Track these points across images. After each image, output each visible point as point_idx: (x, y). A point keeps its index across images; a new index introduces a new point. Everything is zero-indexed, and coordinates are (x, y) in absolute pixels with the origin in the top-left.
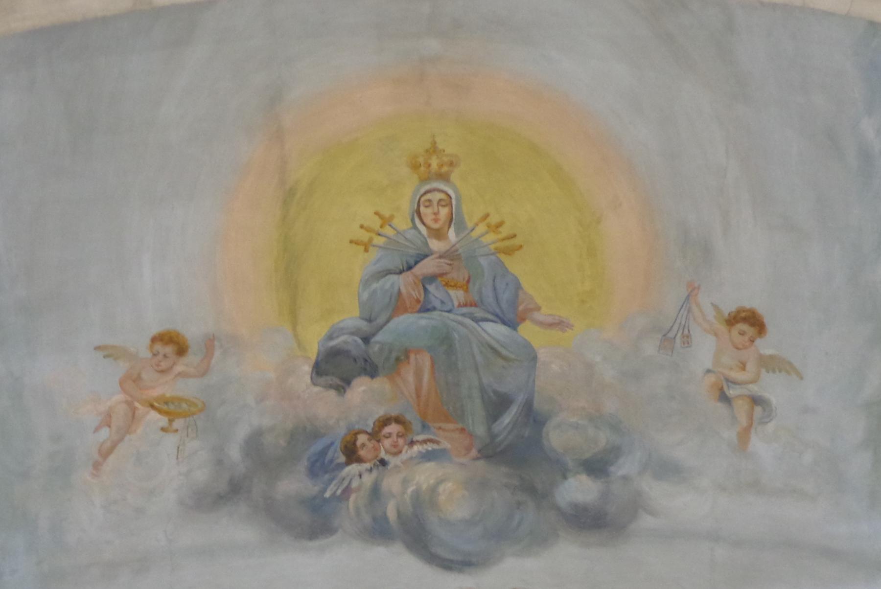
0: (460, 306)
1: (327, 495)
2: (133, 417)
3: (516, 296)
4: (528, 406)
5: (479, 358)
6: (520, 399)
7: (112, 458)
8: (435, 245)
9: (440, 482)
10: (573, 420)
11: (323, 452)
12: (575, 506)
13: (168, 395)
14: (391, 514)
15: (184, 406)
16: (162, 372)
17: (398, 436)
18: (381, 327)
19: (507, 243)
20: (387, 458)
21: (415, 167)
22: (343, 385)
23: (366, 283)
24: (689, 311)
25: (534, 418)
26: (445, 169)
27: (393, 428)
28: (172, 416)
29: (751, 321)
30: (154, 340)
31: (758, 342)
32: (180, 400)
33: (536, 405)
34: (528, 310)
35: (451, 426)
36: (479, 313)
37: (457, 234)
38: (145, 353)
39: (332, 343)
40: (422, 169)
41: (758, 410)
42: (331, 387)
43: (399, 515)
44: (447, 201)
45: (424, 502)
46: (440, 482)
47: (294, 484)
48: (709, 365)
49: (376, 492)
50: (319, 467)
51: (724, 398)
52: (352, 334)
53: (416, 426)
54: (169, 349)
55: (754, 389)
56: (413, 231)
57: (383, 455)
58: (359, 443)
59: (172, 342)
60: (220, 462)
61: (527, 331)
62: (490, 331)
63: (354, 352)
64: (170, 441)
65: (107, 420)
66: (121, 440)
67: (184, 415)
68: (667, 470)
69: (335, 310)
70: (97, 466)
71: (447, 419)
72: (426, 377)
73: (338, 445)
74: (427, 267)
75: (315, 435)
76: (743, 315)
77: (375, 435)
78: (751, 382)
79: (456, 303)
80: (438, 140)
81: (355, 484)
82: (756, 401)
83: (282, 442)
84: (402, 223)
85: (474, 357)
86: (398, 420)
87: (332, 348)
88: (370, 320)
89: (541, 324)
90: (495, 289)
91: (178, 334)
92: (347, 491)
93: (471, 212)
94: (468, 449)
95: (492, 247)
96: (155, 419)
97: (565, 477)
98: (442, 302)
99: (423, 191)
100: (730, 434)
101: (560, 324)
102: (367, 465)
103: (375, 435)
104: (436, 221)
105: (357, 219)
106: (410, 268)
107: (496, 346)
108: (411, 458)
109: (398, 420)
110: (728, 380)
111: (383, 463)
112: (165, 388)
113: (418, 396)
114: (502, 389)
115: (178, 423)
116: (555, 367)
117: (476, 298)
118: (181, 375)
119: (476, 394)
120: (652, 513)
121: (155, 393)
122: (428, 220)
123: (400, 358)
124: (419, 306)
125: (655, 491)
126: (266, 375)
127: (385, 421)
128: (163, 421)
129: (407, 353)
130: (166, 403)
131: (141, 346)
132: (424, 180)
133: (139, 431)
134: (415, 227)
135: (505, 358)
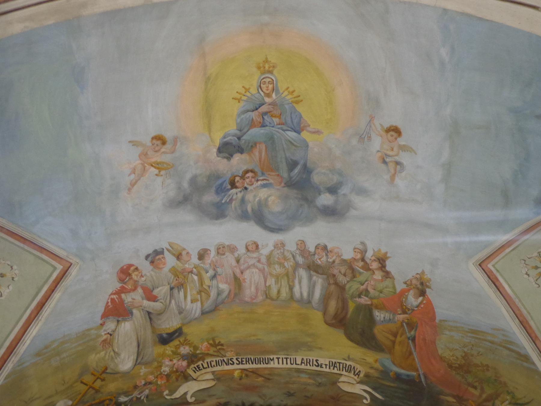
0: (277, 124)
1: (223, 201)
2: (144, 170)
3: (300, 120)
4: (305, 166)
5: (285, 146)
6: (302, 162)
7: (135, 186)
8: (267, 100)
9: (269, 196)
10: (323, 171)
11: (222, 184)
13: (158, 161)
14: (249, 209)
15: (165, 165)
16: (156, 151)
17: (252, 178)
18: (245, 133)
19: (296, 99)
20: (247, 186)
21: (259, 68)
22: (230, 157)
23: (239, 115)
24: (370, 127)
25: (307, 170)
26: (271, 69)
27: (250, 174)
28: (160, 170)
29: (396, 131)
30: (153, 138)
31: (398, 139)
32: (163, 163)
33: (308, 165)
34: (305, 126)
35: (273, 174)
36: (285, 127)
37: (276, 95)
38: (149, 144)
40: (262, 69)
41: (398, 167)
42: (225, 157)
43: (253, 210)
45: (262, 204)
46: (269, 196)
47: (210, 197)
48: (378, 149)
49: (243, 200)
50: (220, 190)
51: (385, 162)
52: (233, 136)
53: (259, 173)
54: (159, 142)
55: (397, 158)
56: (258, 94)
57: (246, 185)
58: (236, 180)
59: (160, 140)
60: (179, 188)
61: (305, 135)
62: (289, 135)
63: (234, 143)
64: (159, 180)
65: (134, 171)
66: (139, 179)
67: (165, 169)
68: (362, 191)
69: (226, 127)
70: (129, 190)
71: (272, 171)
73: (227, 181)
74: (264, 109)
75: (218, 177)
76: (392, 128)
77: (243, 177)
78: (396, 156)
79: (276, 124)
80: (268, 57)
81: (234, 197)
82: (397, 163)
83: (205, 180)
84: (253, 91)
85: (283, 145)
86: (252, 171)
87: (225, 142)
88: (240, 131)
89: (310, 132)
90: (291, 118)
91: (162, 136)
92: (231, 200)
93: (282, 86)
94: (281, 183)
95: (290, 101)
97: (320, 194)
98: (270, 123)
99: (262, 78)
100: (387, 177)
101: (318, 132)
102: (240, 190)
103: (243, 177)
104: (267, 90)
105: (236, 88)
106: (257, 109)
107: (292, 141)
108: (257, 187)
109: (252, 171)
110: (386, 155)
111: (246, 188)
112: (157, 158)
113: (260, 161)
114: (294, 158)
115: (163, 172)
116: (316, 150)
117: (284, 121)
118: (164, 153)
119: (284, 160)
120: (356, 209)
121: (153, 160)
122: (264, 90)
123: (252, 146)
124: (260, 125)
125: (356, 200)
126: (198, 153)
127: (247, 172)
128: (156, 171)
129: (256, 144)
130: (158, 164)
131: (147, 140)
132: (263, 73)
133: (147, 176)
134: (259, 92)
135: (295, 146)
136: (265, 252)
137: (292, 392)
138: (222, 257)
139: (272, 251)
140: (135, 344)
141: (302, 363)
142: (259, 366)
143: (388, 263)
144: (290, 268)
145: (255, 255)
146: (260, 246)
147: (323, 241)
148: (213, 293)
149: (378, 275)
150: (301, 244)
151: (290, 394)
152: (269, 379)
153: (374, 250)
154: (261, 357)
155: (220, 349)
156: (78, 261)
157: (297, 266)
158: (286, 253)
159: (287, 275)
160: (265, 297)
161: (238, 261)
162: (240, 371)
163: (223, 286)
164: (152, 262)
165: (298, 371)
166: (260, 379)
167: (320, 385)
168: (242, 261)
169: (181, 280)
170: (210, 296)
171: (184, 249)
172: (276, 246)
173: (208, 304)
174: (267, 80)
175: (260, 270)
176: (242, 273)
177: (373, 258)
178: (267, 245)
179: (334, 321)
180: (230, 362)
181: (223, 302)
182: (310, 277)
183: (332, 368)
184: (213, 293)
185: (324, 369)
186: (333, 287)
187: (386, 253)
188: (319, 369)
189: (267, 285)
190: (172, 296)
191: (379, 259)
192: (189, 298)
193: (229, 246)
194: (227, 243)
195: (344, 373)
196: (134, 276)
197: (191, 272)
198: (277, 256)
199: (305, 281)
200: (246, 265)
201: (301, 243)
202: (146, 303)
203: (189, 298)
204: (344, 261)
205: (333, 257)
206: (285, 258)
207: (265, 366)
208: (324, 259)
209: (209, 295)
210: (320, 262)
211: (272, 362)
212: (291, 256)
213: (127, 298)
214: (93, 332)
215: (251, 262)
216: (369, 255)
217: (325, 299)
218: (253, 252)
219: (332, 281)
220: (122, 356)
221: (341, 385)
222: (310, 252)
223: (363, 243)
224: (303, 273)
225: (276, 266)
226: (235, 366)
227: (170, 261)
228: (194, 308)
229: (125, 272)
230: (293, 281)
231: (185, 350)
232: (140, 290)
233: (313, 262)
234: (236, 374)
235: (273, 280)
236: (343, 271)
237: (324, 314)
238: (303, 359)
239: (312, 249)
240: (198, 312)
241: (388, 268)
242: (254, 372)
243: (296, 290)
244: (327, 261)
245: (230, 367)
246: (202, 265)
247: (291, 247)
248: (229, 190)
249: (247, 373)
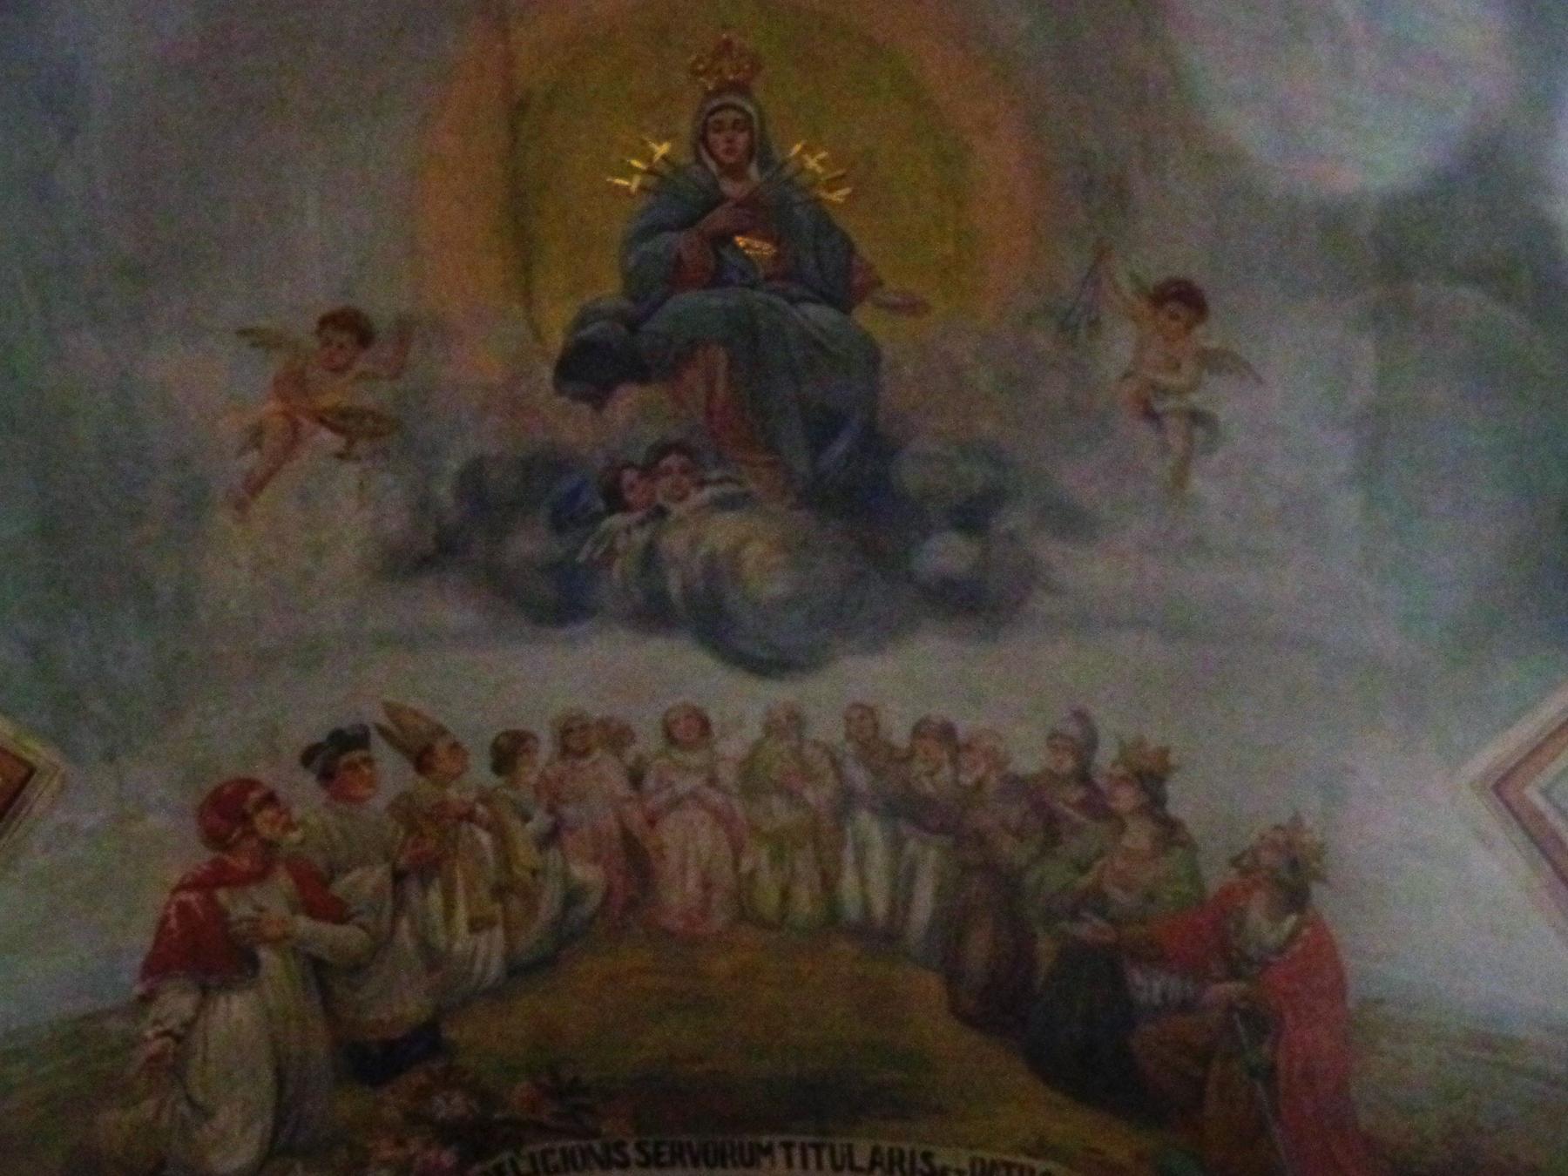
1: (581, 558)
2: (293, 440)
8: (729, 187)
9: (744, 542)
11: (575, 494)
14: (674, 587)
22: (599, 396)
23: (631, 242)
24: (1097, 283)
25: (878, 446)
27: (672, 461)
29: (1182, 300)
31: (1199, 330)
36: (795, 291)
38: (313, 343)
39: (583, 334)
41: (1199, 433)
44: (744, 124)
45: (720, 572)
49: (650, 557)
51: (1151, 415)
54: (345, 337)
55: (1195, 398)
56: (697, 168)
57: (660, 499)
59: (349, 327)
61: (865, 317)
64: (349, 473)
69: (584, 285)
70: (241, 506)
72: (720, 387)
74: (720, 218)
81: (621, 544)
82: (1196, 417)
86: (679, 448)
92: (611, 553)
96: (328, 439)
97: (926, 536)
101: (913, 307)
102: (639, 515)
103: (649, 470)
104: (729, 151)
110: (1154, 386)
113: (710, 413)
115: (362, 446)
118: (362, 376)
121: (328, 400)
127: (663, 450)
131: (304, 329)
134: (699, 160)
136: (732, 747)
139: (758, 746)
140: (267, 1076)
143: (1172, 789)
145: (695, 759)
146: (715, 730)
147: (940, 710)
149: (1139, 835)
150: (863, 722)
156: (56, 760)
157: (847, 800)
158: (808, 751)
161: (636, 778)
163: (585, 872)
164: (326, 776)
168: (650, 783)
169: (430, 845)
171: (442, 731)
172: (770, 728)
173: (532, 938)
174: (731, 116)
175: (716, 814)
176: (652, 823)
177: (1120, 770)
178: (740, 724)
182: (896, 844)
184: (550, 901)
190: (400, 904)
191: (1139, 775)
192: (461, 915)
193: (604, 724)
194: (597, 713)
196: (264, 821)
197: (470, 816)
199: (878, 857)
200: (664, 797)
201: (862, 718)
202: (303, 924)
203: (461, 915)
204: (1017, 785)
205: (975, 765)
206: (808, 774)
209: (531, 900)
210: (929, 788)
212: (825, 764)
213: (239, 906)
214: (115, 1025)
215: (684, 785)
216: (1106, 757)
217: (953, 923)
218: (688, 746)
220: (222, 1118)
223: (1081, 716)
224: (869, 826)
225: (776, 802)
227: (391, 773)
228: (482, 953)
229: (229, 811)
231: (451, 1106)
232: (283, 881)
238: (876, 1151)
240: (496, 969)
241: (1175, 809)
243: (849, 884)
244: (957, 782)
247: (827, 728)
248: (599, 517)
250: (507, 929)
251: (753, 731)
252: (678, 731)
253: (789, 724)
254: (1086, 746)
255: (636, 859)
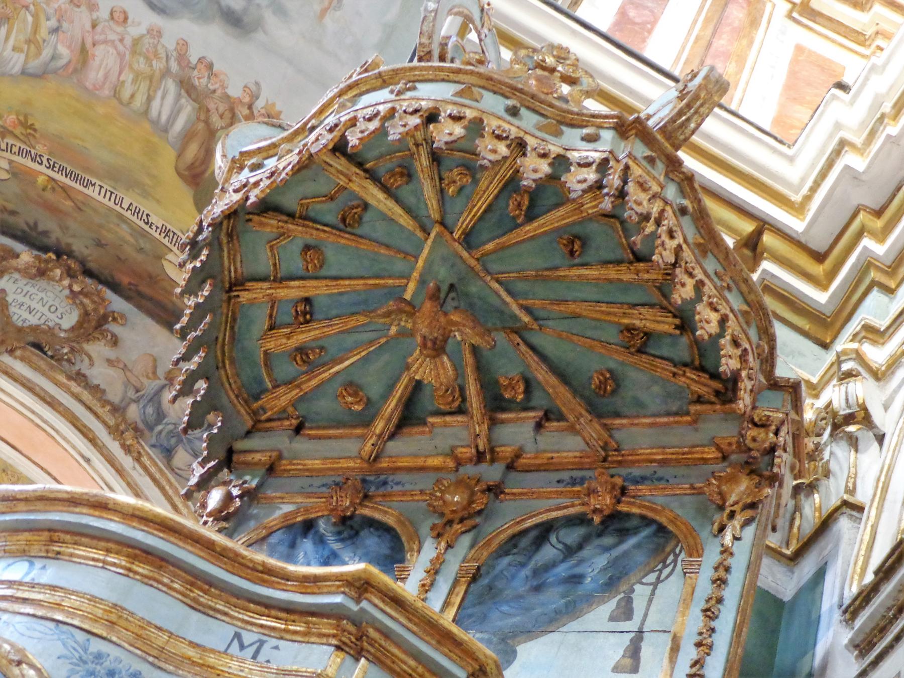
12: (229, 8)
100: (317, 8)
120: (265, 32)
125: (271, 20)
137: (103, 242)
138: (77, 9)
139: (143, 36)
141: (128, 209)
142: (73, 184)
144: (158, 72)
145: (119, 29)
146: (130, 21)
147: (211, 57)
148: (47, 53)
150: (183, 46)
151: (99, 244)
152: (79, 209)
153: (267, 101)
154: (81, 173)
155: (30, 134)
157: (166, 73)
158: (159, 47)
159: (151, 78)
160: (112, 93)
161: (94, 26)
162: (47, 178)
163: (63, 50)
165: (120, 217)
166: (69, 203)
167: (141, 250)
168: (99, 29)
169: (8, 11)
170: (40, 54)
172: (149, 31)
173: (35, 64)
175: (118, 53)
176: (94, 45)
177: (263, 111)
178: (139, 24)
179: (186, 173)
180: (38, 159)
181: (55, 72)
182: (178, 97)
183: (163, 235)
184: (47, 53)
185: (152, 232)
186: (201, 126)
187: (280, 112)
188: (146, 227)
189: (121, 79)
195: (175, 249)
197: (27, 8)
198: (147, 46)
200: (102, 37)
203: (11, 42)
206: (156, 54)
207: (81, 188)
208: (204, 81)
209: (39, 53)
210: (197, 84)
211: (91, 188)
212: (163, 55)
215: (112, 36)
217: (187, 136)
219: (202, 117)
221: (165, 263)
222: (189, 62)
223: (257, 84)
224: (171, 86)
225: (142, 60)
226: (42, 168)
228: (14, 60)
230: (155, 91)
233: (189, 78)
234: (41, 179)
235: (131, 76)
236: (221, 109)
237: (179, 156)
238: (131, 204)
239: (194, 60)
240: (17, 69)
242: (65, 189)
243: (156, 104)
244: (207, 86)
245: (35, 166)
246: (45, 6)
247: (169, 43)
249: (55, 186)
250: (27, 55)
251: (142, 30)
252: (116, 15)
253: (156, 33)
254: (255, 97)
255: (84, 54)
